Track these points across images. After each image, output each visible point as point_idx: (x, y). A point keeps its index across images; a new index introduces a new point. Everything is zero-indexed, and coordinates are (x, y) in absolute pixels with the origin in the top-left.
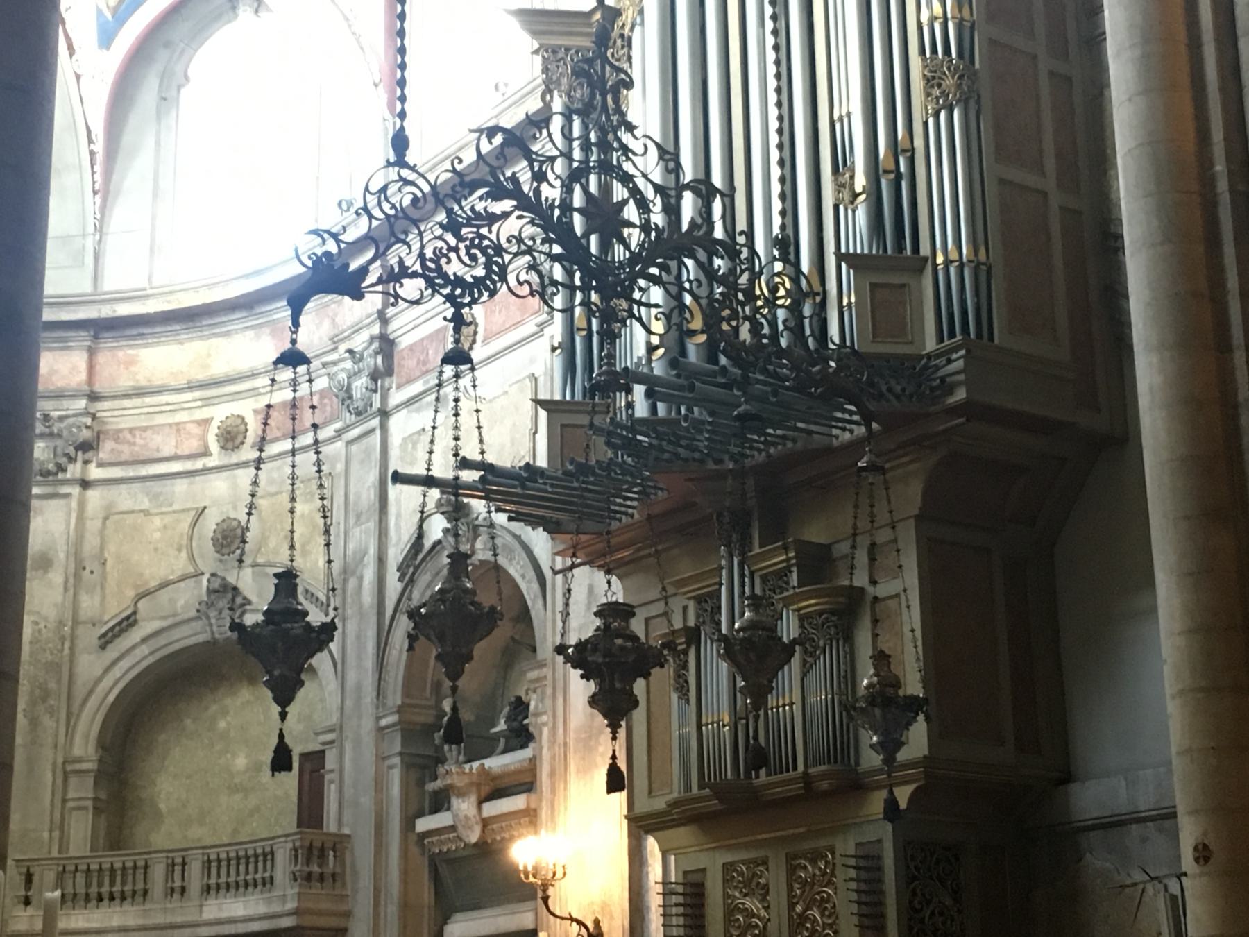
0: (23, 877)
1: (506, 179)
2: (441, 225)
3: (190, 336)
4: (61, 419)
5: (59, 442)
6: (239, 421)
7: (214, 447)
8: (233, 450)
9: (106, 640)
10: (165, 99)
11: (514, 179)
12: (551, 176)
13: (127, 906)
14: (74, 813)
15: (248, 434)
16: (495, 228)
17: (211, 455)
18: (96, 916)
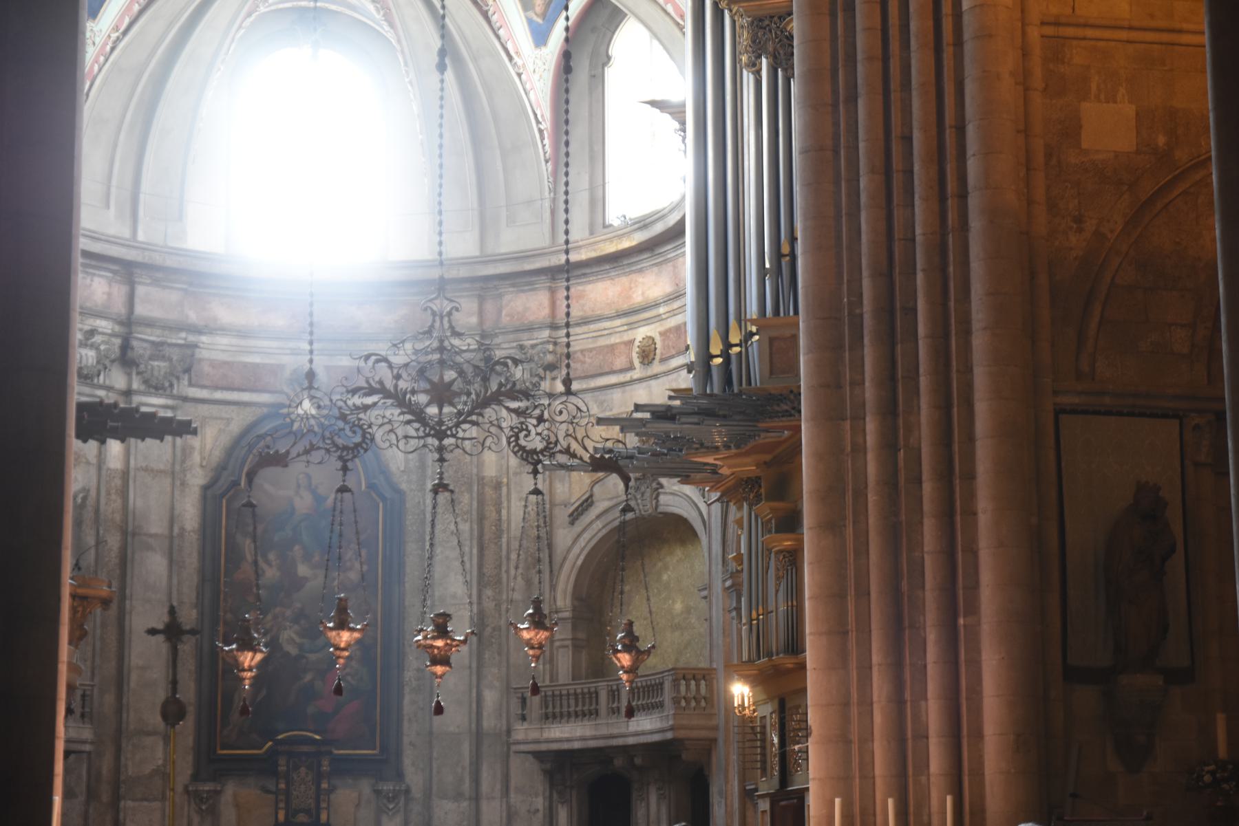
0: (520, 700)
1: (377, 382)
2: (337, 418)
3: (617, 273)
4: (533, 346)
5: (533, 365)
6: (651, 342)
7: (637, 362)
8: (648, 365)
9: (574, 517)
10: (594, 76)
11: (381, 382)
12: (404, 375)
13: (586, 722)
14: (561, 650)
15: (657, 351)
16: (368, 413)
17: (635, 369)
18: (566, 729)
